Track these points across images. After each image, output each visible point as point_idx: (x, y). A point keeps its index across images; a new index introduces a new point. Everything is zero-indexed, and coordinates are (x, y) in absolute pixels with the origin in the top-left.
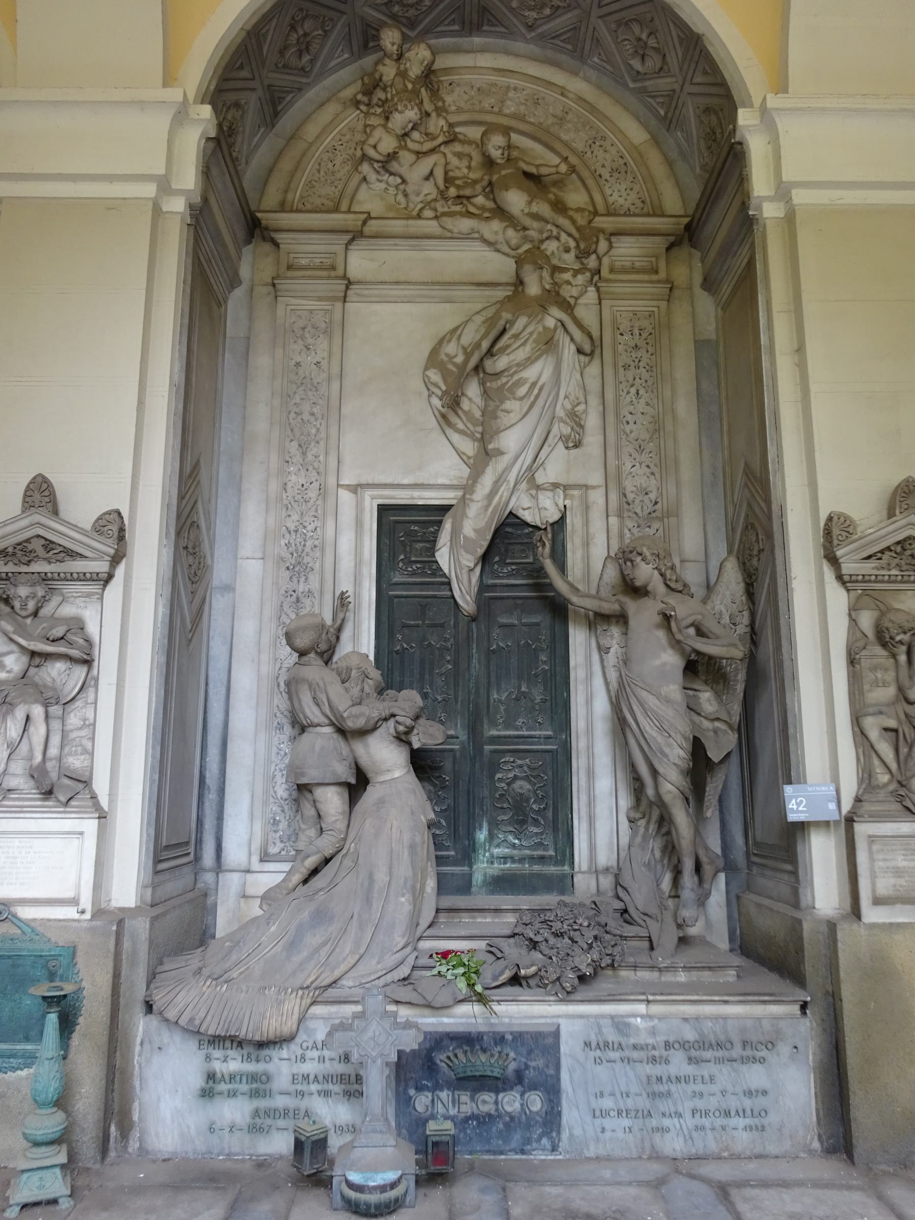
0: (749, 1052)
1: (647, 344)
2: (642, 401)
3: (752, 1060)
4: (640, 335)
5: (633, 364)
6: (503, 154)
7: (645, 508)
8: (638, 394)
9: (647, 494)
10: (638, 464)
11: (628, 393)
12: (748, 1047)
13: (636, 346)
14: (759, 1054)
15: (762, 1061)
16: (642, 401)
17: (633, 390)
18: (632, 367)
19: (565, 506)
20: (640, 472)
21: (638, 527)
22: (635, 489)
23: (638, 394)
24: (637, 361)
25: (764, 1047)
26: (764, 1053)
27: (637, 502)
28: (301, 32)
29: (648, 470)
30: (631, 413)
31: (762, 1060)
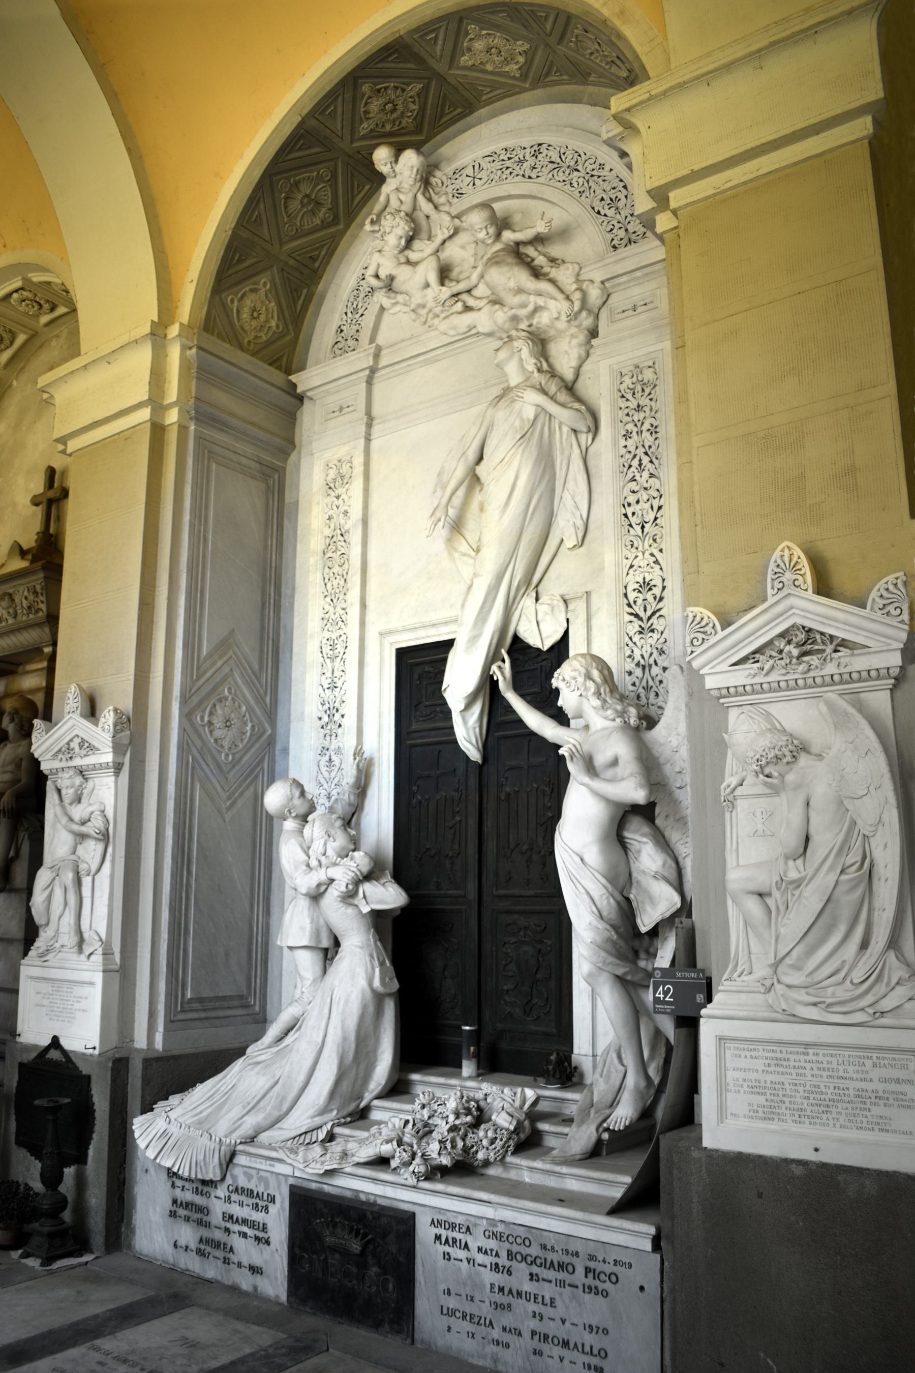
0: (590, 1281)
1: (651, 400)
2: (646, 474)
3: (594, 1290)
4: (643, 390)
5: (635, 430)
6: (488, 234)
7: (648, 607)
8: (640, 465)
9: (650, 589)
10: (640, 554)
11: (630, 466)
12: (591, 1275)
13: (638, 406)
14: (601, 1286)
15: (605, 1294)
16: (646, 474)
17: (635, 463)
18: (634, 434)
19: (568, 620)
21: (640, 633)
22: (637, 586)
23: (640, 465)
24: (639, 424)
25: (607, 1279)
26: (608, 1286)
27: (639, 601)
28: (300, 196)
30: (633, 492)
31: (605, 1293)
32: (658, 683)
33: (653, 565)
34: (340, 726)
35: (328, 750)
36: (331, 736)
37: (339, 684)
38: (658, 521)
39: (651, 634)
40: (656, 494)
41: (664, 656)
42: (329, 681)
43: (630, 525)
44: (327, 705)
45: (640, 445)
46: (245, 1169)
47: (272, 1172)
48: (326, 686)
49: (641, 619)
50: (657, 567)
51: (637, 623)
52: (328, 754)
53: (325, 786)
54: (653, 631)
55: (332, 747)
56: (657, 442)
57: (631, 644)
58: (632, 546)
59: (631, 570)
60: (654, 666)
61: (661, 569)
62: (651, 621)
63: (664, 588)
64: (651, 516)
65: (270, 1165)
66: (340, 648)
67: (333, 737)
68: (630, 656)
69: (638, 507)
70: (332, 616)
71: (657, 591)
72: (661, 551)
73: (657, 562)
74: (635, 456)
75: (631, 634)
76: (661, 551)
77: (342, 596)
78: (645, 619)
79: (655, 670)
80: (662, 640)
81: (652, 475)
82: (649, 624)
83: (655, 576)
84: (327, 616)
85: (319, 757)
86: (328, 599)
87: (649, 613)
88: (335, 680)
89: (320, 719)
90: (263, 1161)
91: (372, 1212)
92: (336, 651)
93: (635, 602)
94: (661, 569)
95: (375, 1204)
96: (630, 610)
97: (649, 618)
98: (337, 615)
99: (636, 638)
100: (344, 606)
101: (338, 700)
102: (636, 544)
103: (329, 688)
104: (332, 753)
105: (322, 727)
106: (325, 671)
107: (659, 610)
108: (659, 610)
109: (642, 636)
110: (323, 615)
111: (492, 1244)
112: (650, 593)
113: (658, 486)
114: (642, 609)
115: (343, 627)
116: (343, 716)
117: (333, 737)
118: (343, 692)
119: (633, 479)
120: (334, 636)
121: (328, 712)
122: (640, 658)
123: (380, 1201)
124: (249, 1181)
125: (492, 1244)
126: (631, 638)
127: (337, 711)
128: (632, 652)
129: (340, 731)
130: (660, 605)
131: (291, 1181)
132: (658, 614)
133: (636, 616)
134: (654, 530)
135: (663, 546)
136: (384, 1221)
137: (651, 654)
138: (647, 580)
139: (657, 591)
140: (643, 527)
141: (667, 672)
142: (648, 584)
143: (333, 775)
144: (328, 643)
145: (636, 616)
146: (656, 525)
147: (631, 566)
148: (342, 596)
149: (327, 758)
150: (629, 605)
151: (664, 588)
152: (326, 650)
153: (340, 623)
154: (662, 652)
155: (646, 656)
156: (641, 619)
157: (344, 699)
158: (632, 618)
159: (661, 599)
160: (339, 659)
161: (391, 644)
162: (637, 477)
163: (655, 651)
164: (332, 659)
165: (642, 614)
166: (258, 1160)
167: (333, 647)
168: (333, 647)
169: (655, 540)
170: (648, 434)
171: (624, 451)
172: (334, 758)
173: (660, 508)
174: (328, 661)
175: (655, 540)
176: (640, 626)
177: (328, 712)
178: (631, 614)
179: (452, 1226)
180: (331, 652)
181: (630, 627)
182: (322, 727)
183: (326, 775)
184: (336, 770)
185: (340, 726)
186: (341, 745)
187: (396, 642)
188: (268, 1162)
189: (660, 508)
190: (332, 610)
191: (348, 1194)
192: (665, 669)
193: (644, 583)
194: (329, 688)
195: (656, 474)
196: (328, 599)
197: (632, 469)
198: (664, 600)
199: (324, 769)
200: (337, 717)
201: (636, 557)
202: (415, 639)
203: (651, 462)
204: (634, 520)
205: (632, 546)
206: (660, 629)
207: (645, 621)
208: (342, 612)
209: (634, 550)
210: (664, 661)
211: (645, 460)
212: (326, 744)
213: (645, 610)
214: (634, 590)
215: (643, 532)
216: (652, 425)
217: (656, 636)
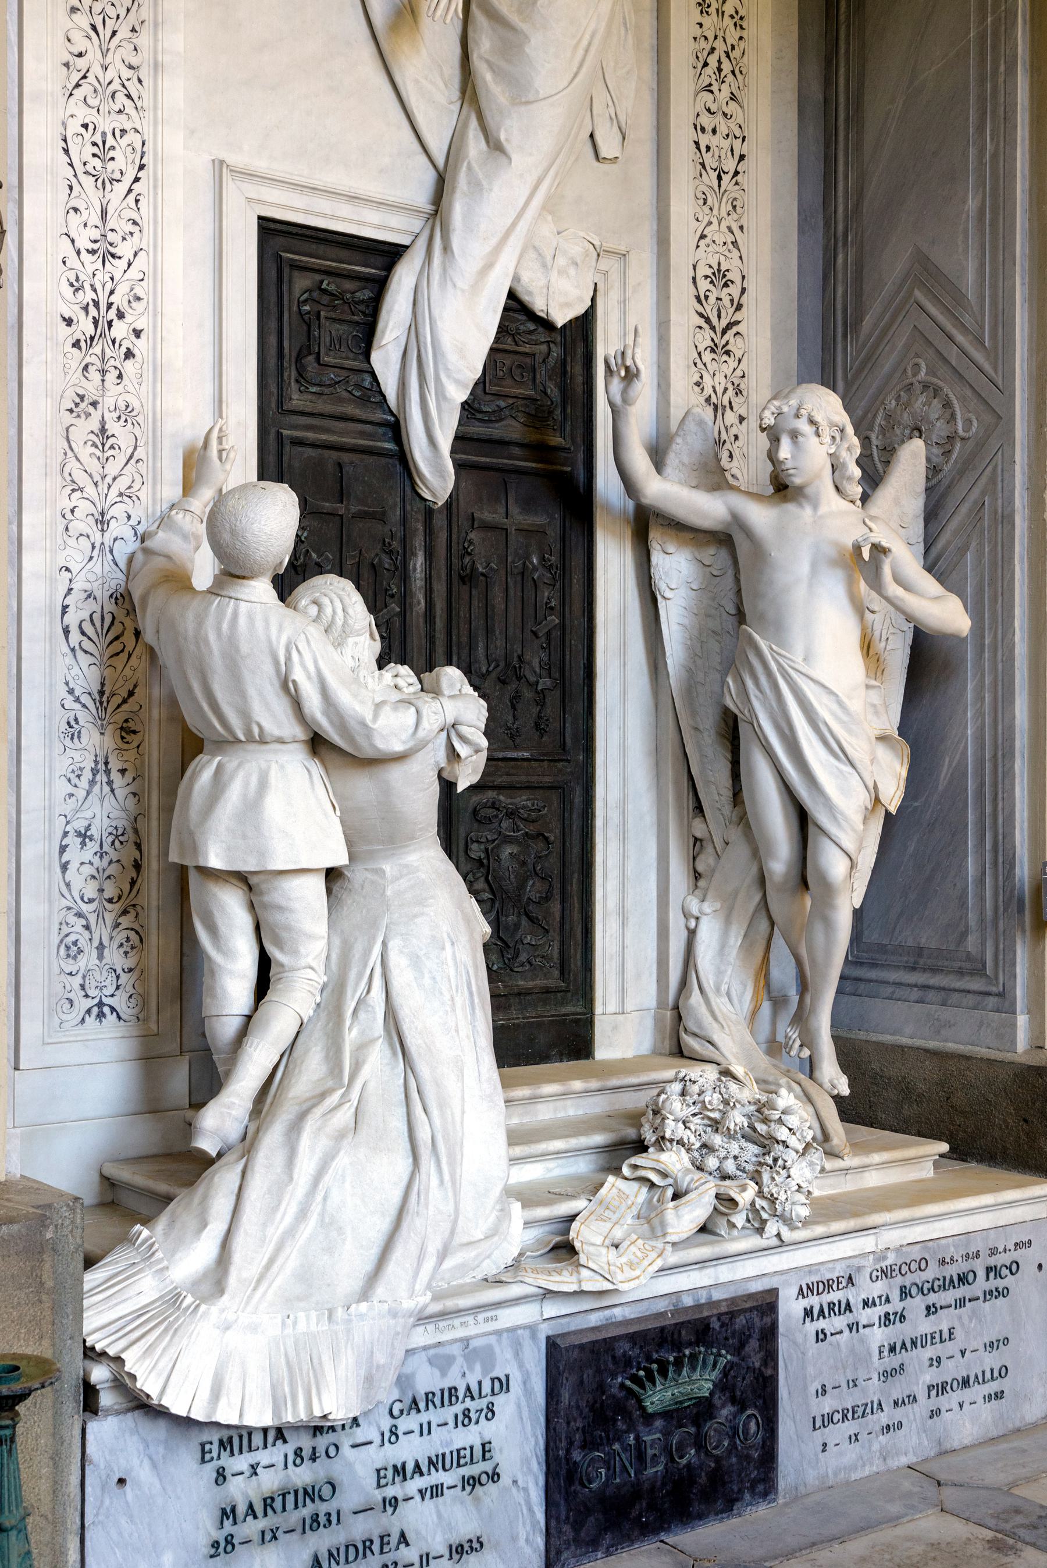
7: (723, 314)
9: (726, 285)
10: (715, 221)
11: (706, 64)
20: (720, 240)
21: (713, 351)
22: (709, 272)
27: (712, 299)
29: (730, 238)
32: (733, 438)
33: (731, 246)
34: (129, 354)
35: (94, 404)
36: (104, 372)
37: (125, 250)
38: (739, 178)
39: (725, 358)
40: (738, 133)
41: (740, 399)
42: (96, 234)
43: (703, 165)
44: (90, 295)
45: (720, 34)
46: (432, 1352)
47: (498, 1333)
48: (83, 243)
49: (713, 328)
50: (735, 253)
51: (708, 333)
52: (96, 415)
53: (90, 490)
54: (728, 353)
55: (109, 401)
56: (742, 43)
57: (700, 365)
58: (705, 201)
59: (702, 243)
60: (728, 409)
61: (741, 258)
62: (726, 337)
63: (743, 290)
64: (730, 165)
65: (486, 1320)
66: (123, 162)
67: (111, 377)
68: (698, 384)
69: (714, 141)
70: (96, 69)
71: (735, 290)
72: (741, 228)
73: (735, 243)
74: (713, 49)
75: (701, 348)
76: (741, 228)
77: (124, 33)
78: (719, 330)
79: (730, 417)
80: (739, 373)
81: (733, 97)
82: (723, 342)
83: (731, 265)
84: (81, 63)
85: (69, 419)
86: (82, 20)
87: (724, 322)
88: (111, 237)
89: (69, 322)
90: (470, 1319)
91: (719, 1316)
92: (111, 165)
93: (706, 297)
94: (741, 258)
95: (712, 1304)
96: (701, 309)
97: (724, 332)
98: (111, 74)
99: (707, 357)
100: (134, 62)
101: (122, 290)
102: (709, 202)
103: (93, 252)
104: (110, 417)
105: (76, 344)
106: (81, 205)
107: (737, 323)
108: (737, 323)
109: (714, 356)
110: (67, 57)
111: (878, 1288)
112: (726, 290)
113: (740, 121)
114: (715, 313)
115: (133, 112)
116: (137, 333)
117: (111, 377)
118: (134, 273)
119: (708, 89)
120: (106, 124)
121: (93, 311)
122: (711, 391)
123: (717, 1295)
124: (444, 1373)
125: (878, 1288)
126: (699, 354)
127: (121, 315)
128: (701, 377)
129: (129, 366)
130: (738, 317)
131: (545, 1330)
132: (735, 329)
133: (708, 320)
134: (733, 191)
135: (744, 222)
136: (740, 1321)
137: (726, 389)
138: (723, 269)
139: (735, 290)
140: (719, 178)
141: (745, 423)
142: (724, 276)
143: (112, 468)
144: (87, 136)
145: (708, 320)
146: (737, 184)
147: (703, 237)
148: (124, 33)
149: (96, 426)
150: (699, 301)
151: (743, 290)
152: (81, 151)
153: (120, 97)
154: (738, 392)
155: (720, 391)
156: (713, 328)
157: (139, 291)
158: (701, 322)
159: (739, 307)
160: (121, 188)
161: (249, 200)
162: (715, 88)
163: (730, 387)
164: (105, 183)
165: (714, 320)
166: (457, 1322)
167: (102, 150)
168: (102, 150)
169: (734, 207)
170: (731, 23)
171: (698, 32)
172: (112, 427)
173: (742, 157)
174: (88, 182)
175: (734, 207)
176: (713, 340)
177: (93, 311)
178: (701, 315)
179: (828, 1286)
180: (97, 162)
181: (699, 336)
182: (76, 344)
183: (94, 466)
184: (122, 459)
185: (129, 354)
186: (135, 403)
187: (261, 202)
188: (481, 1317)
189: (742, 157)
190: (94, 55)
191: (661, 1306)
192: (742, 419)
193: (719, 271)
194: (93, 252)
195: (740, 99)
196: (82, 20)
197: (709, 71)
198: (744, 309)
199: (85, 452)
200: (120, 330)
201: (710, 223)
202: (306, 212)
203: (733, 72)
204: (708, 158)
205: (705, 201)
206: (739, 354)
207: (719, 334)
208: (126, 73)
209: (706, 209)
210: (741, 405)
211: (726, 67)
212: (91, 387)
213: (719, 317)
214: (706, 277)
215: (720, 186)
216: (737, 12)
217: (732, 363)
